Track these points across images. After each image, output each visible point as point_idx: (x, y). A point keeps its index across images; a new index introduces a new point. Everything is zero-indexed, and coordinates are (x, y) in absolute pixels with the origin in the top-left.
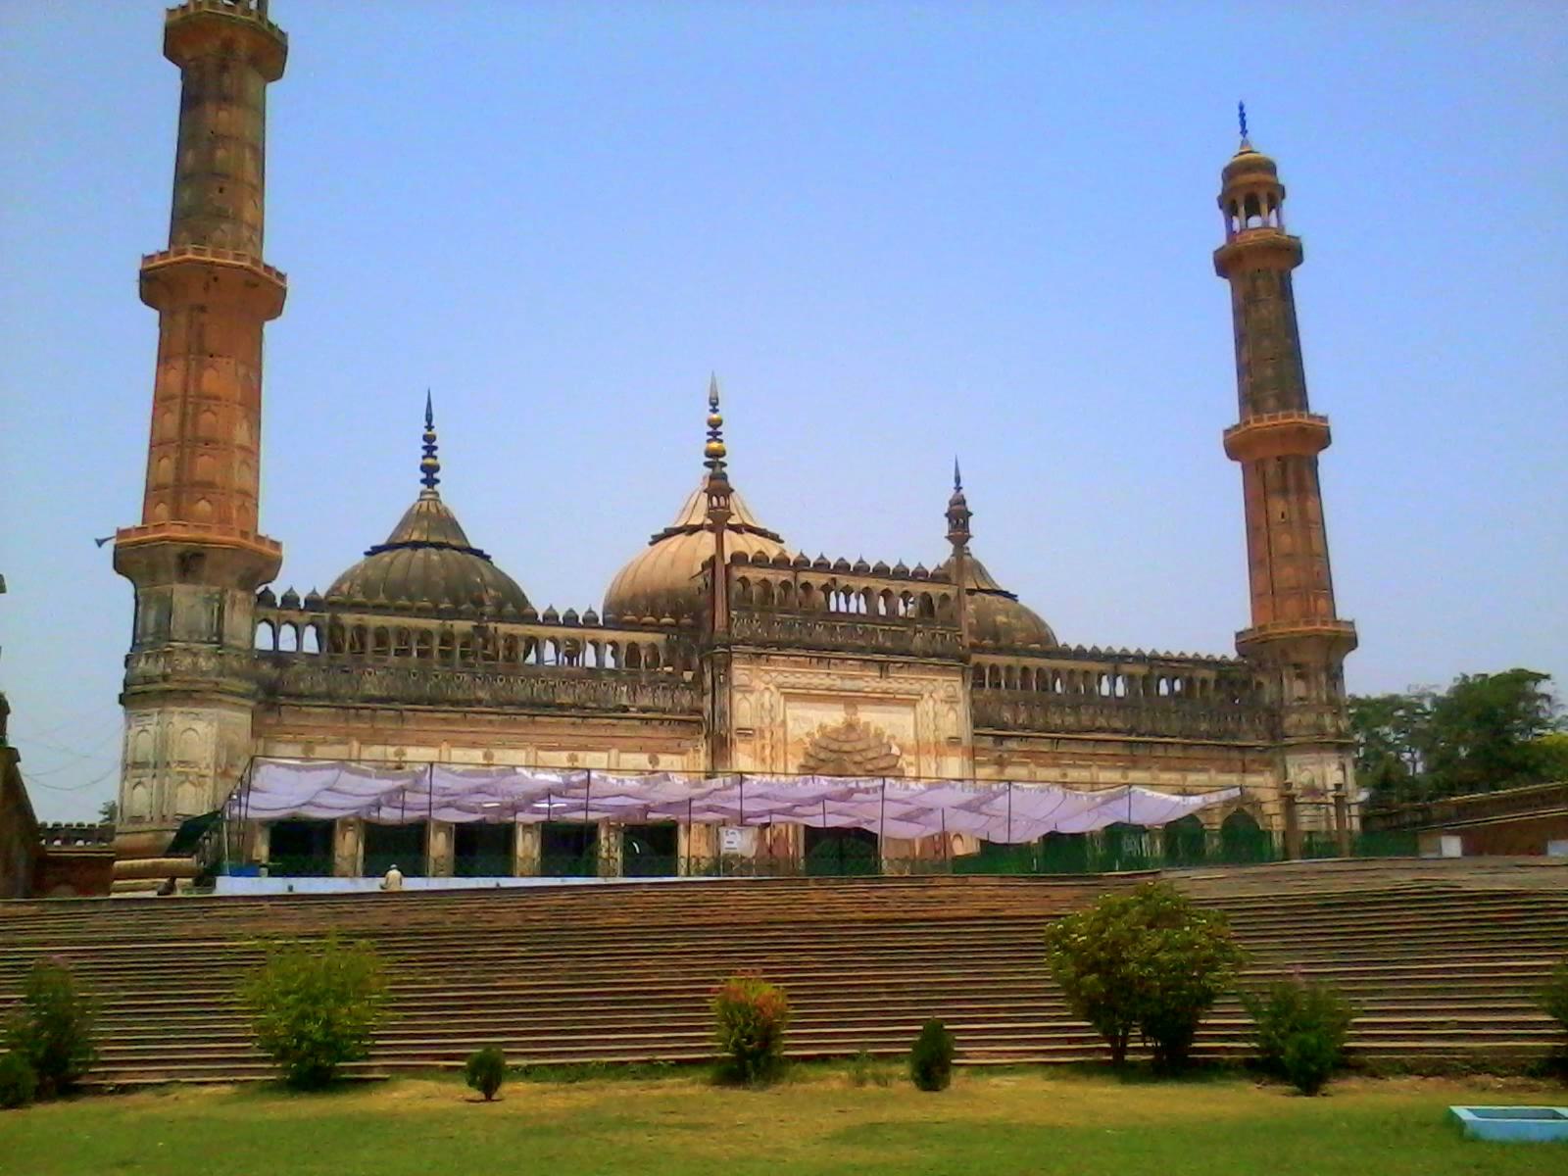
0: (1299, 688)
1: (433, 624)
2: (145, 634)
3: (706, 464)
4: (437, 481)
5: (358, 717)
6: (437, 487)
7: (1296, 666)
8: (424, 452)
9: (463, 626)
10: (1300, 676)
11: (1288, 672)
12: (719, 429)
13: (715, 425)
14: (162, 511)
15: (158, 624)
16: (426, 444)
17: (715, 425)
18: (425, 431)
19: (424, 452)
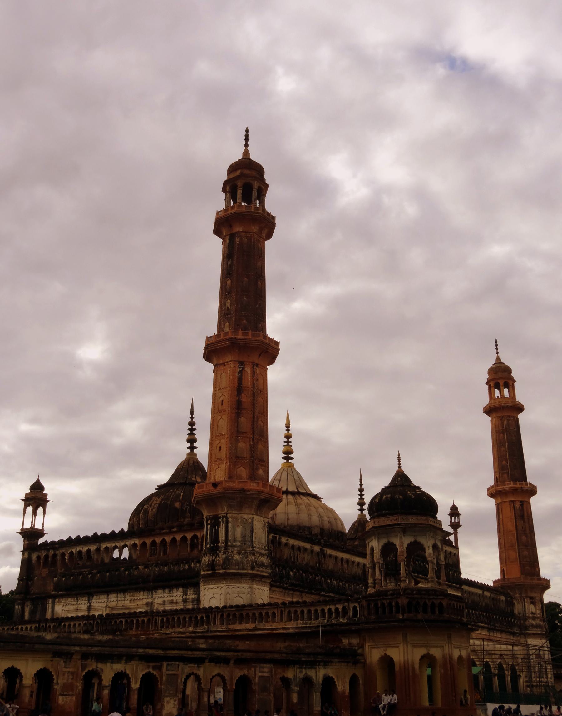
0: (531, 608)
1: (308, 546)
2: (235, 541)
3: (283, 458)
4: (196, 448)
5: (288, 594)
6: (195, 451)
7: (531, 598)
8: (189, 432)
9: (317, 548)
10: (532, 603)
11: (527, 600)
12: (290, 440)
13: (288, 437)
14: (243, 472)
15: (244, 537)
16: (190, 427)
17: (288, 437)
18: (190, 420)
19: (189, 432)
